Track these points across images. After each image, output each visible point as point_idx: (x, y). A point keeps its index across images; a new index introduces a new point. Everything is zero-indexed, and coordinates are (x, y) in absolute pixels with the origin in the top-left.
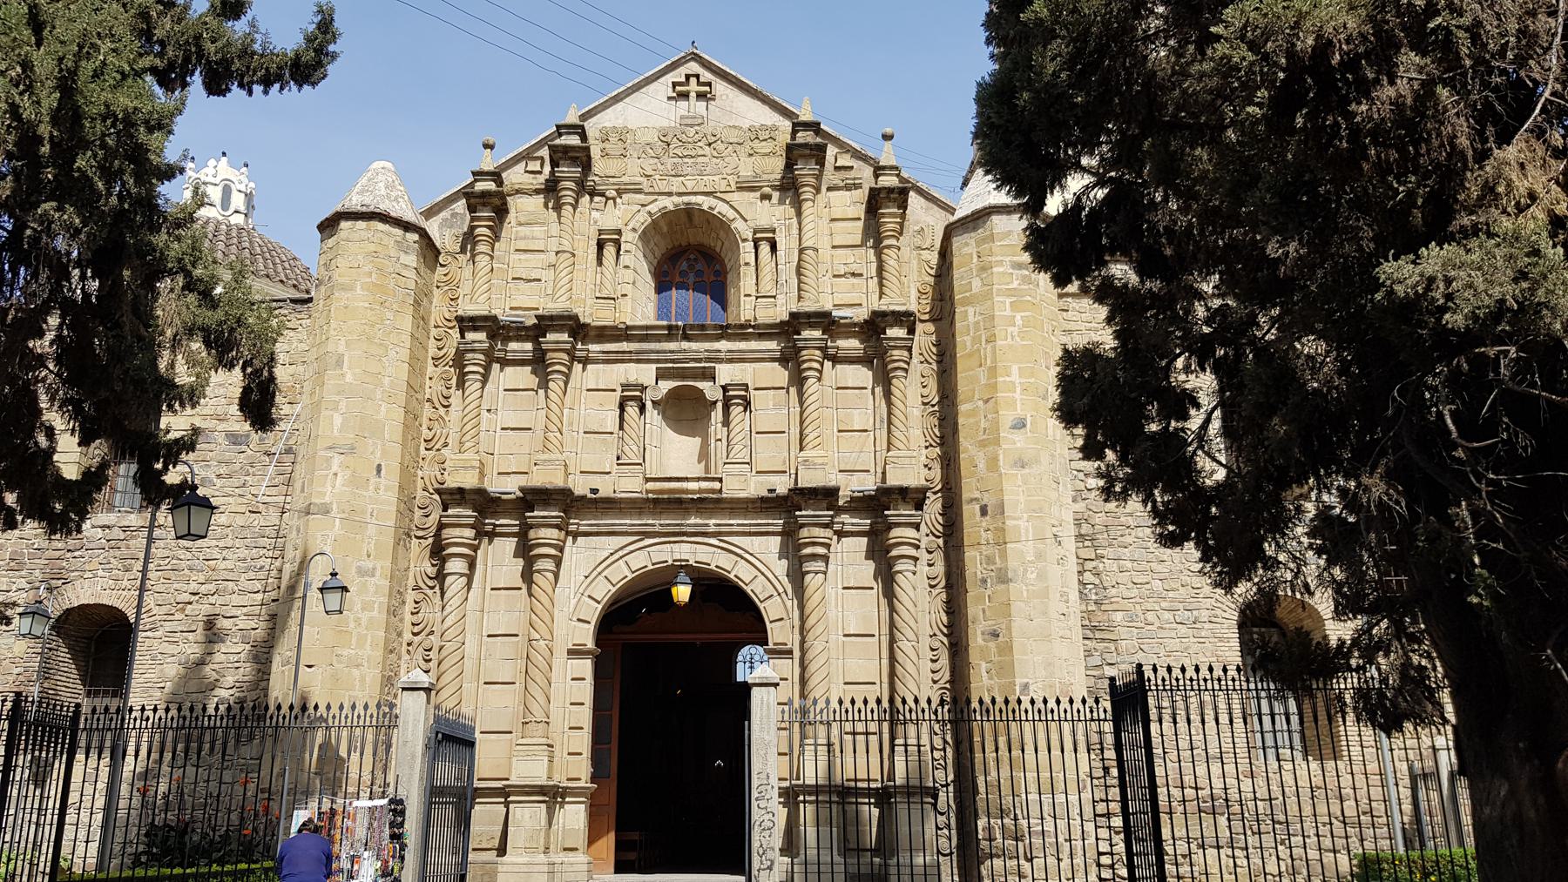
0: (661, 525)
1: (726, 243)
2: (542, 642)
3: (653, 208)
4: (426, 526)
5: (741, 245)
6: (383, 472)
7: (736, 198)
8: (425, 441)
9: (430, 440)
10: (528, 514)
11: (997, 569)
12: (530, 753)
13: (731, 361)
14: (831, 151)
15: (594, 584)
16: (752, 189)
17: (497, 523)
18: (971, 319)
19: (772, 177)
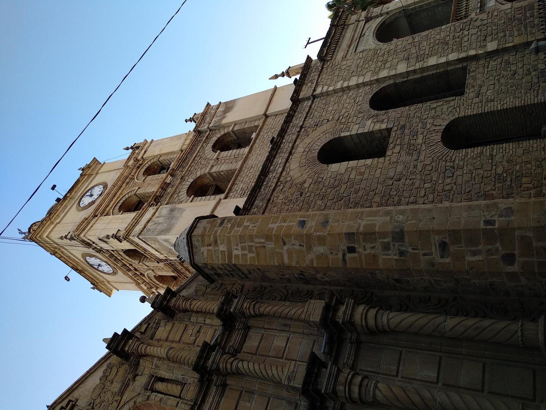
5: (150, 402)
11: (393, 241)
14: (138, 334)
16: (127, 385)
19: (128, 371)
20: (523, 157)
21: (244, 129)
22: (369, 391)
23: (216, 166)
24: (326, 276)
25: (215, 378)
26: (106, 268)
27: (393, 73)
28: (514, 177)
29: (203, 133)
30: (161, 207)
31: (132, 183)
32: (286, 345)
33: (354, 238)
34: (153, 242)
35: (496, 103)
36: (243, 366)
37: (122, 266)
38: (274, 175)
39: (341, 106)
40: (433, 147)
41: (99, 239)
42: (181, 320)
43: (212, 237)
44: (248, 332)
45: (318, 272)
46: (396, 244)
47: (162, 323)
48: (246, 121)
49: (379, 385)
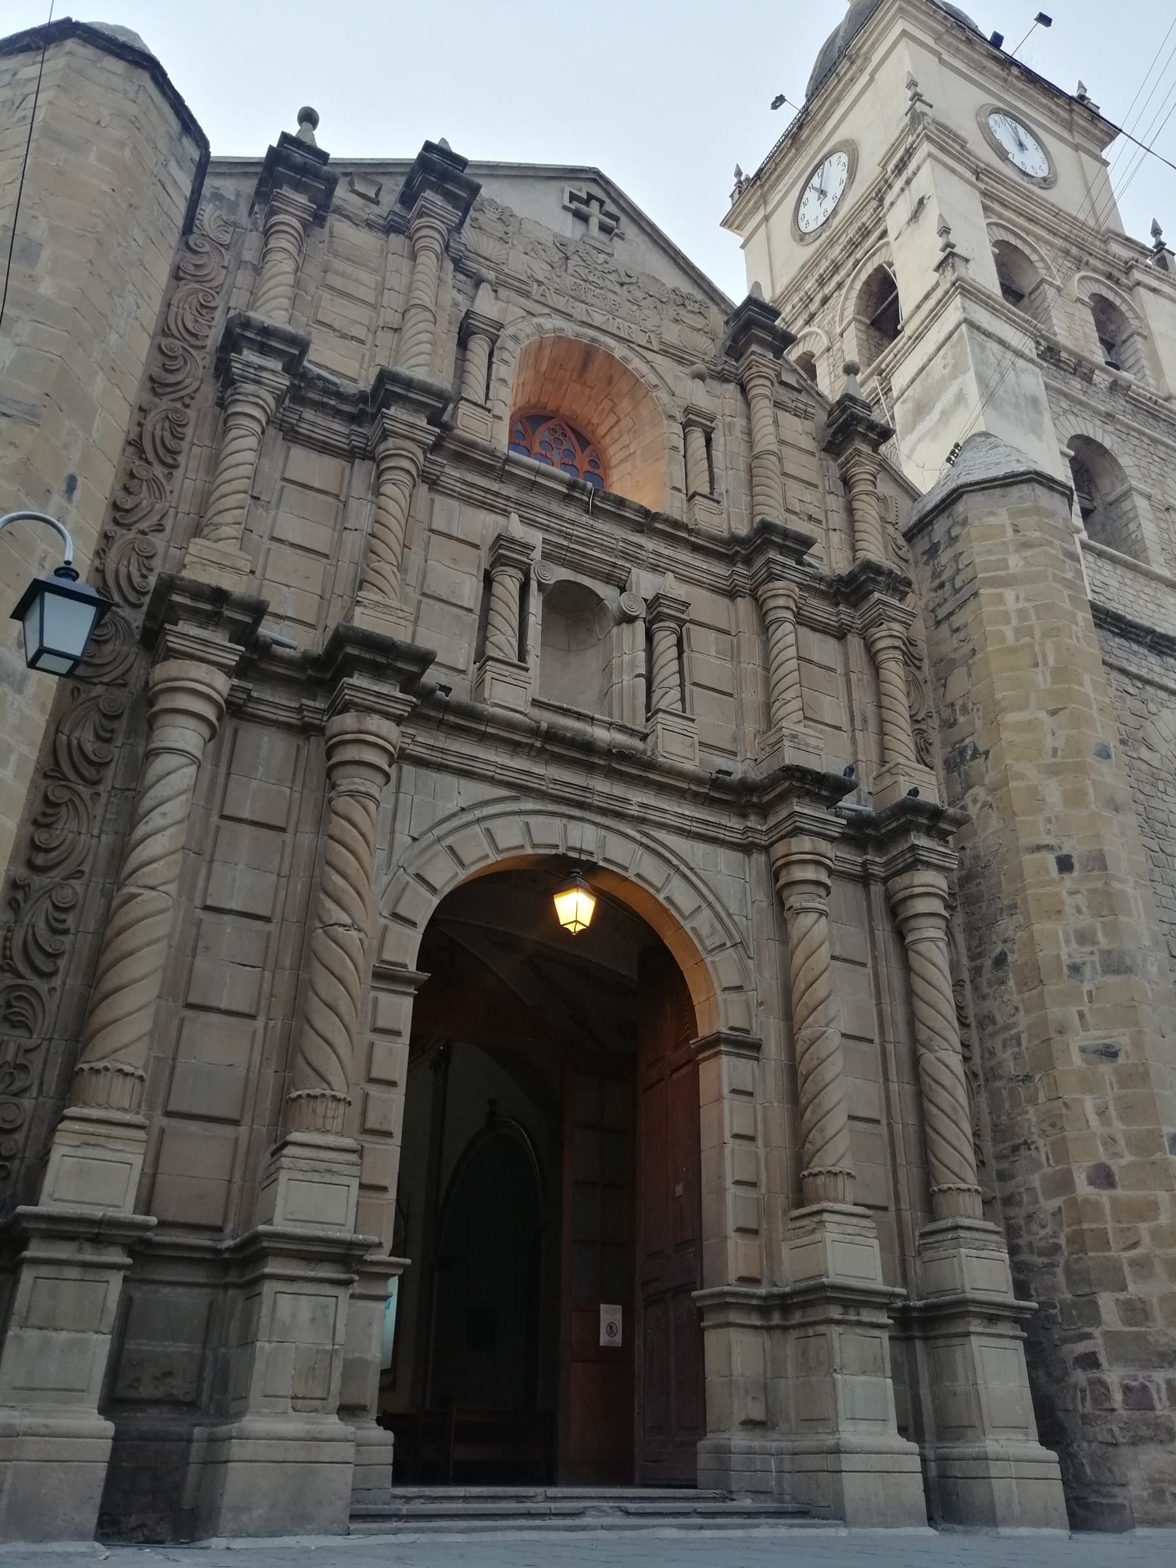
0: (555, 781)
1: (626, 422)
2: (353, 933)
4: (96, 661)
6: (77, 494)
7: (658, 360)
8: (115, 506)
9: (127, 511)
10: (350, 681)
11: (1102, 952)
12: (321, 1166)
13: (655, 568)
15: (427, 855)
16: (681, 361)
17: (255, 694)
19: (707, 359)
22: (813, 901)
23: (1149, 508)
24: (982, 808)
25: (740, 568)
26: (814, 213)
30: (1037, 370)
31: (1069, 264)
32: (827, 725)
33: (1093, 869)
34: (951, 362)
36: (786, 633)
38: (1157, 669)
41: (921, 202)
43: (1038, 534)
44: (833, 636)
45: (991, 790)
46: (1096, 958)
47: (809, 425)
49: (824, 918)
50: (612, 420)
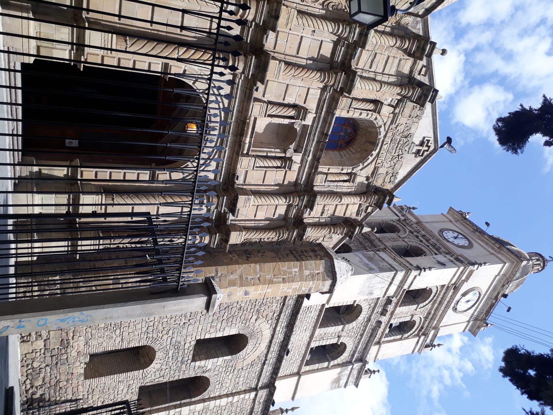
1: (353, 156)
3: (382, 129)
7: (372, 167)
13: (302, 161)
16: (373, 173)
18: (294, 270)
19: (374, 182)
20: (103, 340)
21: (319, 363)
23: (339, 331)
26: (449, 235)
27: (192, 407)
28: (109, 327)
29: (359, 360)
31: (426, 314)
34: (384, 267)
35: (118, 379)
37: (430, 239)
38: (283, 325)
39: (233, 380)
40: (161, 347)
41: (444, 265)
42: (339, 218)
45: (236, 260)
48: (318, 370)
50: (354, 152)
